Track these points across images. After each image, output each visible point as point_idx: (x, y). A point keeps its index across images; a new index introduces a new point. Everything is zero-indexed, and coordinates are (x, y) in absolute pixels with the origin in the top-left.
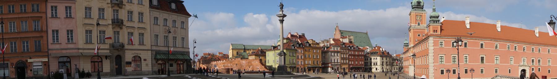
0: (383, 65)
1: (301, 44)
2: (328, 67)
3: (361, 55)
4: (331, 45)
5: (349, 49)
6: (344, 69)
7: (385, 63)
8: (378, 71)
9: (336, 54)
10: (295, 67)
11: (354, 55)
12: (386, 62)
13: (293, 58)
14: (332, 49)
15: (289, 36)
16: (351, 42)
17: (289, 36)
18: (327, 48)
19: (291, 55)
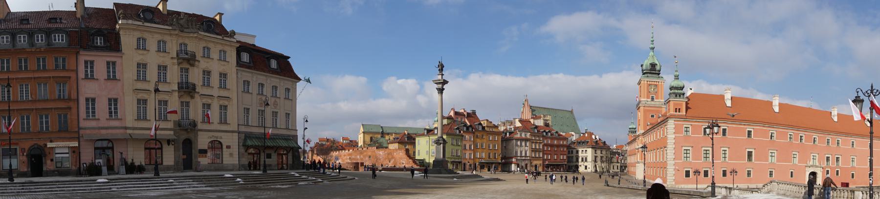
0: (595, 161)
1: (471, 126)
2: (511, 163)
3: (563, 146)
4: (516, 128)
5: (543, 136)
6: (536, 166)
7: (599, 159)
8: (589, 170)
9: (523, 144)
10: (460, 162)
11: (552, 146)
12: (602, 157)
13: (458, 148)
14: (518, 136)
15: (452, 114)
16: (547, 125)
17: (452, 114)
18: (511, 133)
19: (455, 143)
